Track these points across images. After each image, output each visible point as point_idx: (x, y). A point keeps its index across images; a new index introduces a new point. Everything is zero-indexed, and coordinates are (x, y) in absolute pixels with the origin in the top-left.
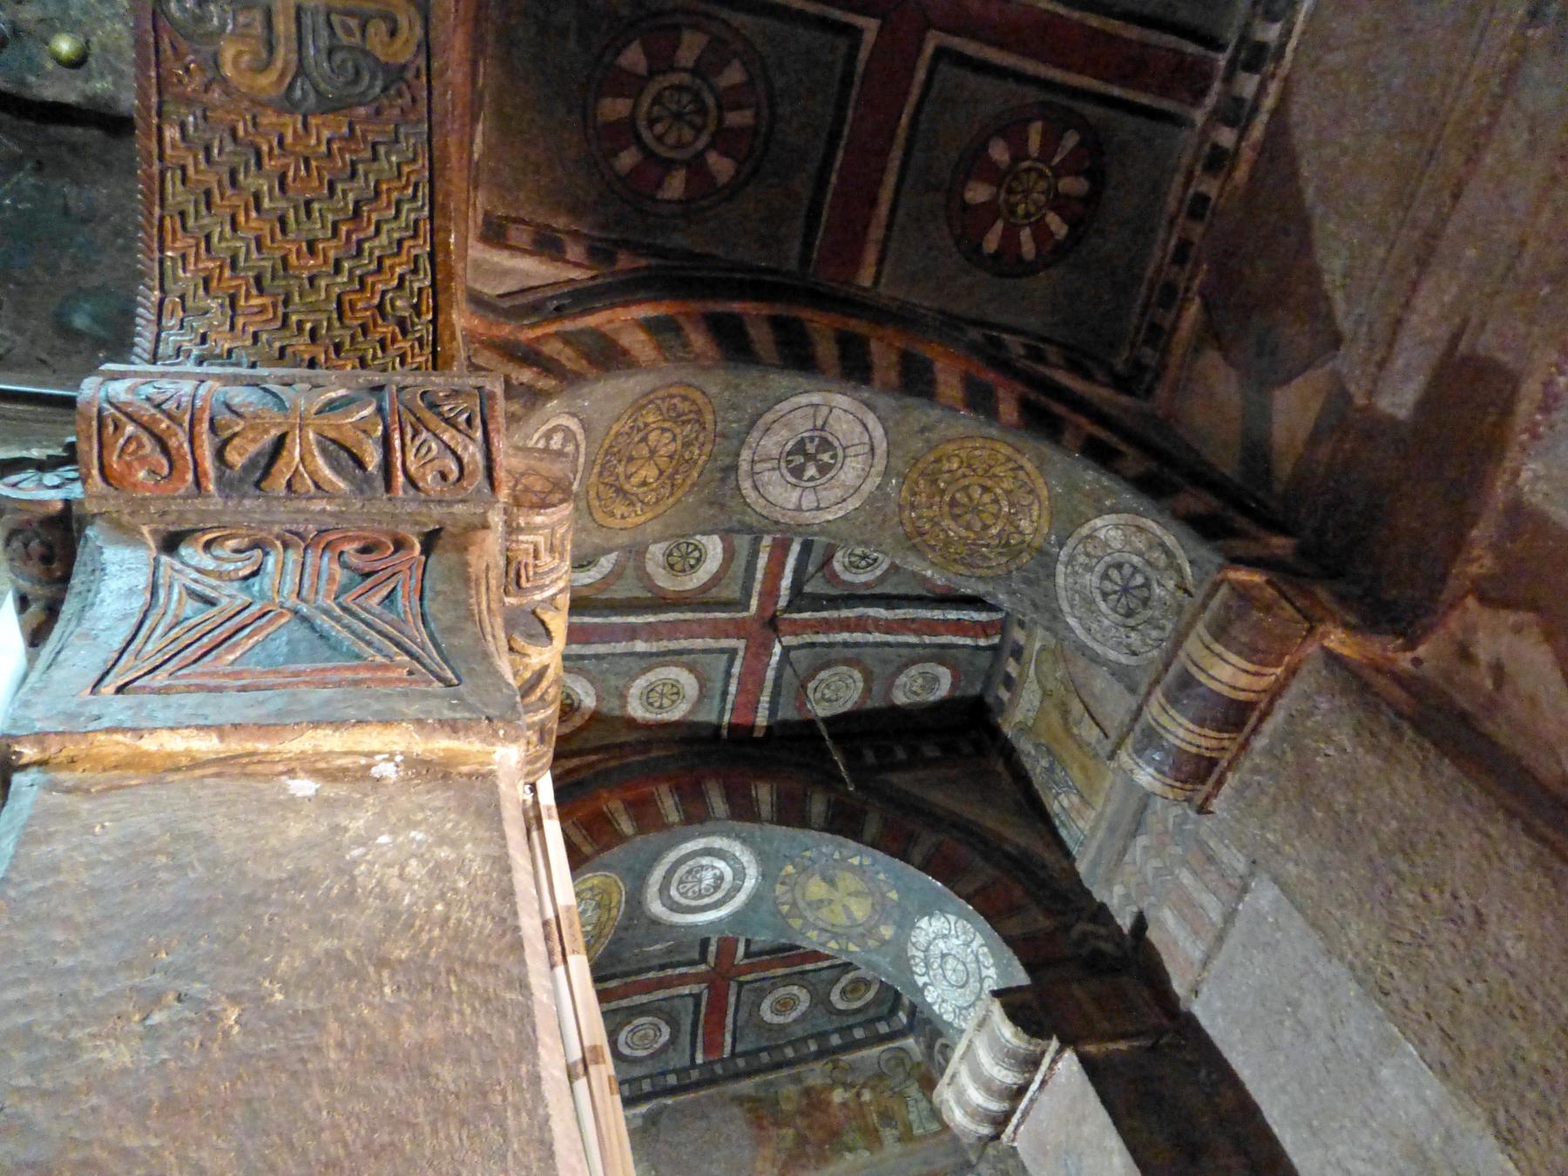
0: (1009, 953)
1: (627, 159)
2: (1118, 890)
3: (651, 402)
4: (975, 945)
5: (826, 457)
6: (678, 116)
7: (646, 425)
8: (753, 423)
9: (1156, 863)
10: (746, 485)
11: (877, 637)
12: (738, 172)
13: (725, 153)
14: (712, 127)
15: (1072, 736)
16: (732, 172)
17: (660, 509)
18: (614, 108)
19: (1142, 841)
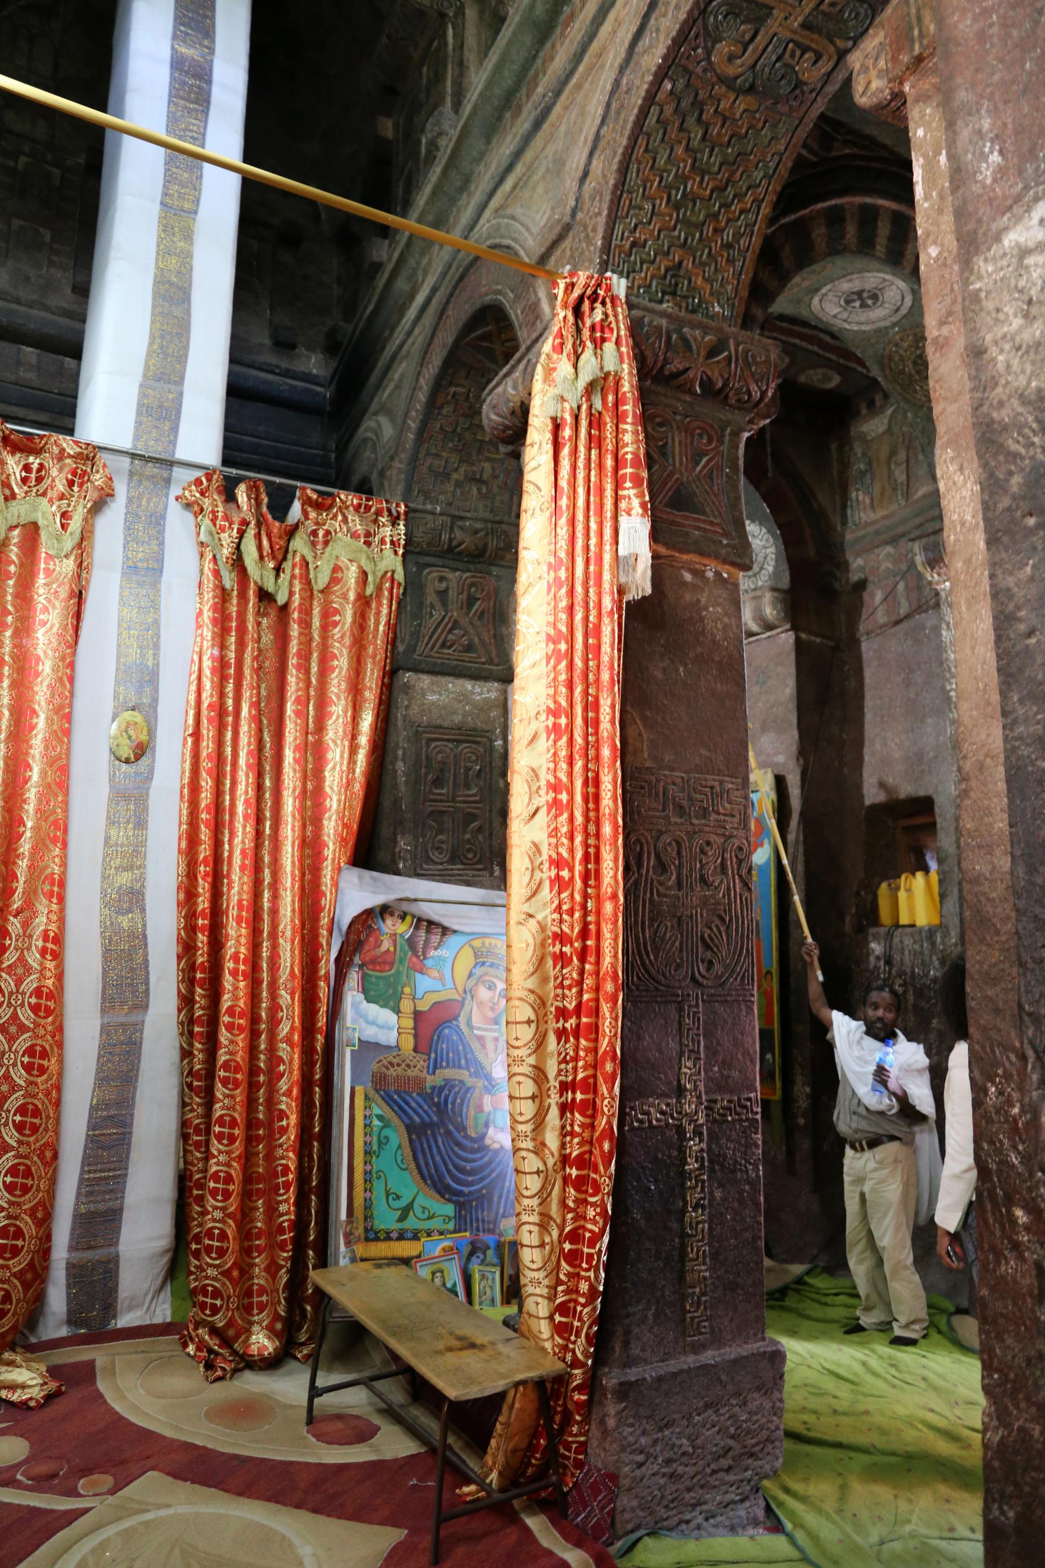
0: (785, 567)
2: (860, 561)
4: (769, 550)
5: (870, 302)
8: (844, 276)
9: (889, 565)
11: (815, 349)
15: (889, 468)
19: (889, 549)
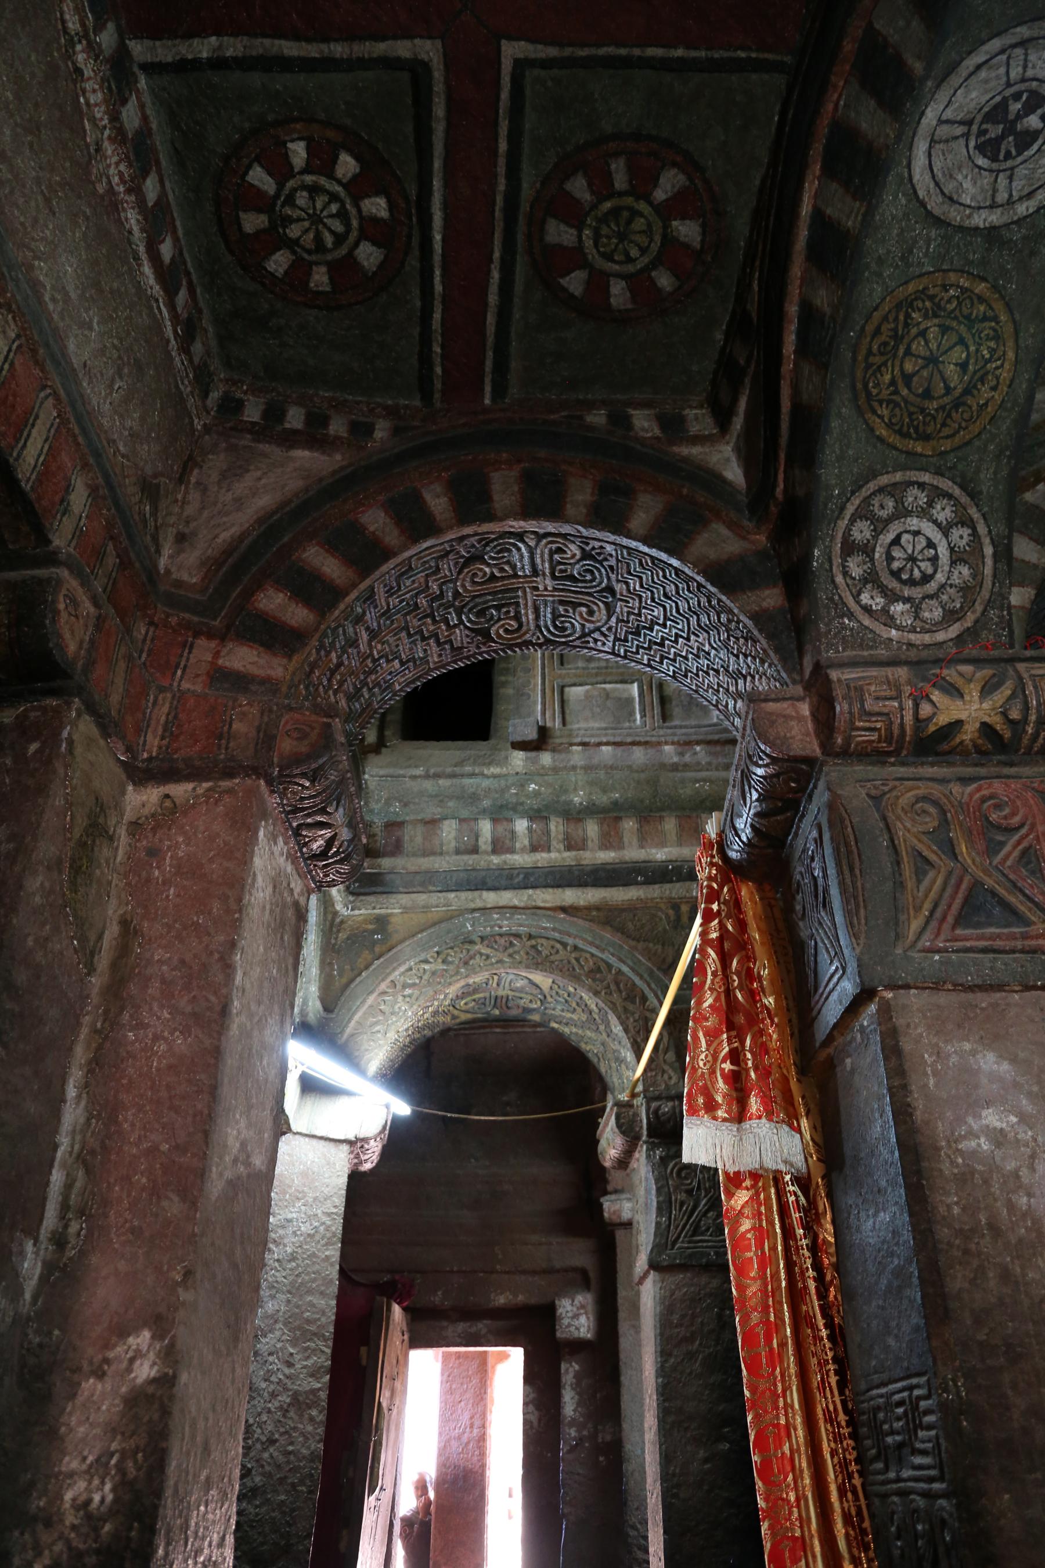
1: (665, 281)
3: (866, 386)
6: (622, 237)
7: (893, 382)
8: (938, 222)
10: (1022, 209)
12: (674, 164)
13: (655, 183)
14: (629, 200)
16: (674, 171)
17: (1008, 329)
18: (618, 293)
